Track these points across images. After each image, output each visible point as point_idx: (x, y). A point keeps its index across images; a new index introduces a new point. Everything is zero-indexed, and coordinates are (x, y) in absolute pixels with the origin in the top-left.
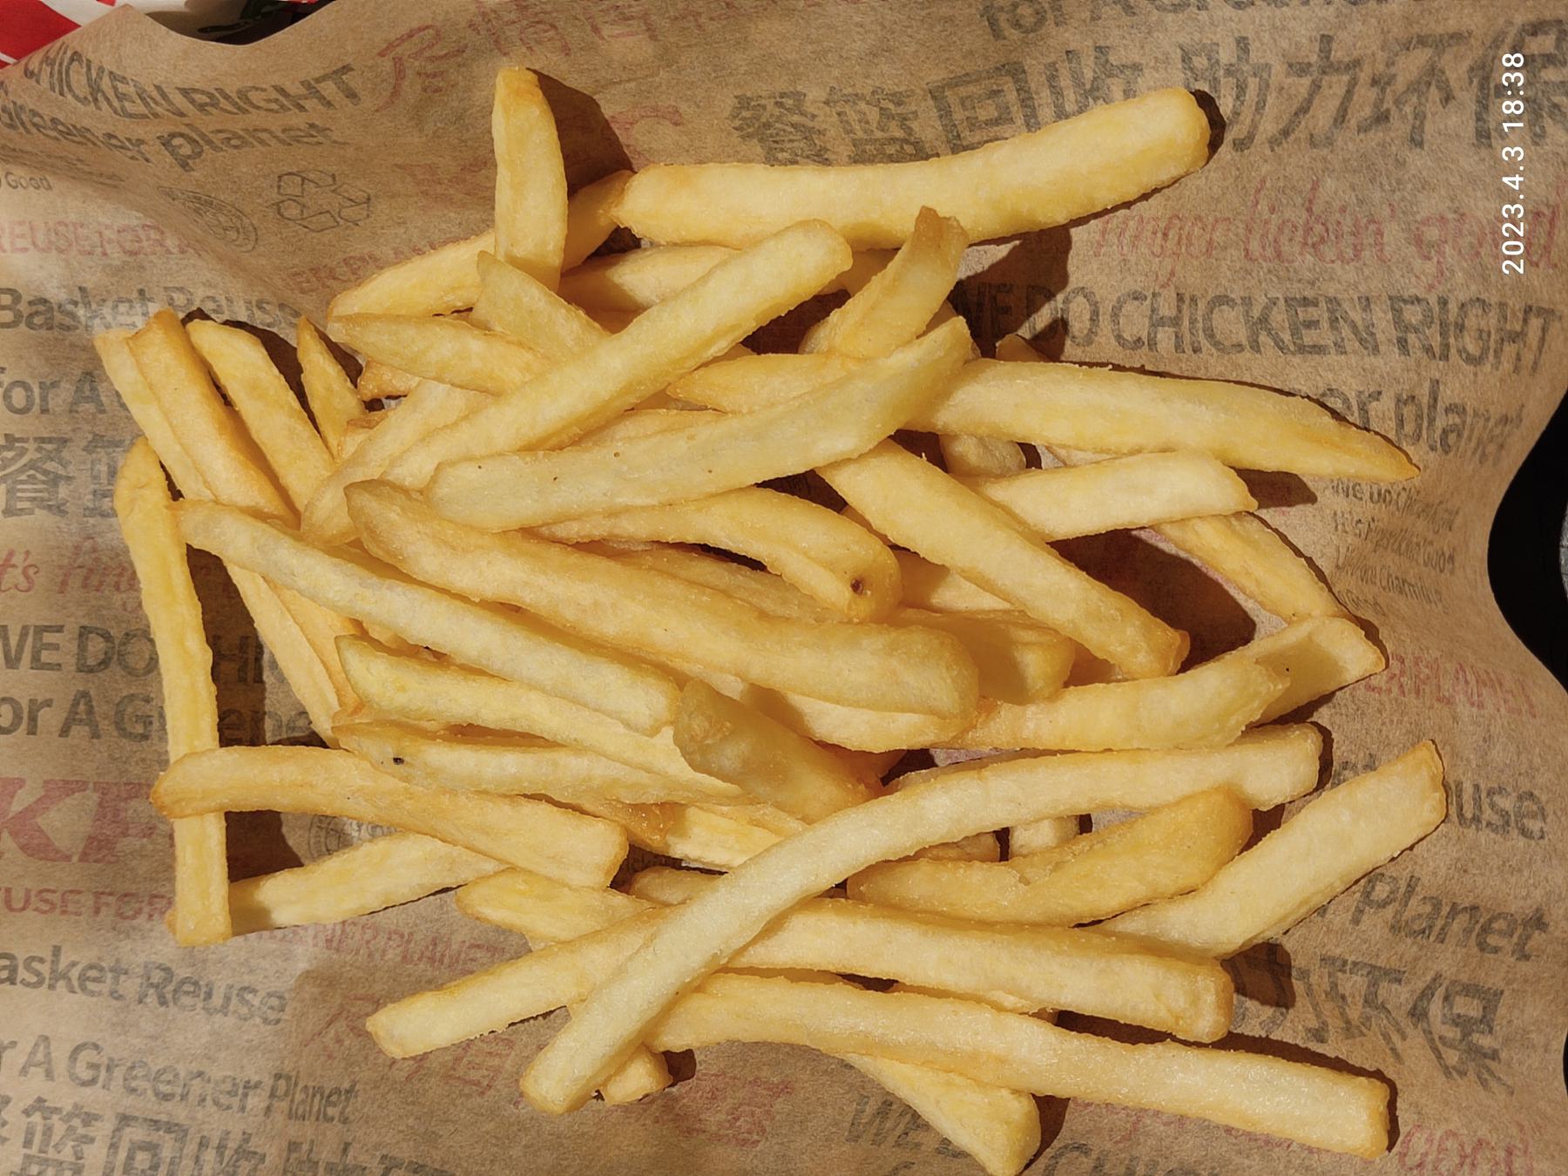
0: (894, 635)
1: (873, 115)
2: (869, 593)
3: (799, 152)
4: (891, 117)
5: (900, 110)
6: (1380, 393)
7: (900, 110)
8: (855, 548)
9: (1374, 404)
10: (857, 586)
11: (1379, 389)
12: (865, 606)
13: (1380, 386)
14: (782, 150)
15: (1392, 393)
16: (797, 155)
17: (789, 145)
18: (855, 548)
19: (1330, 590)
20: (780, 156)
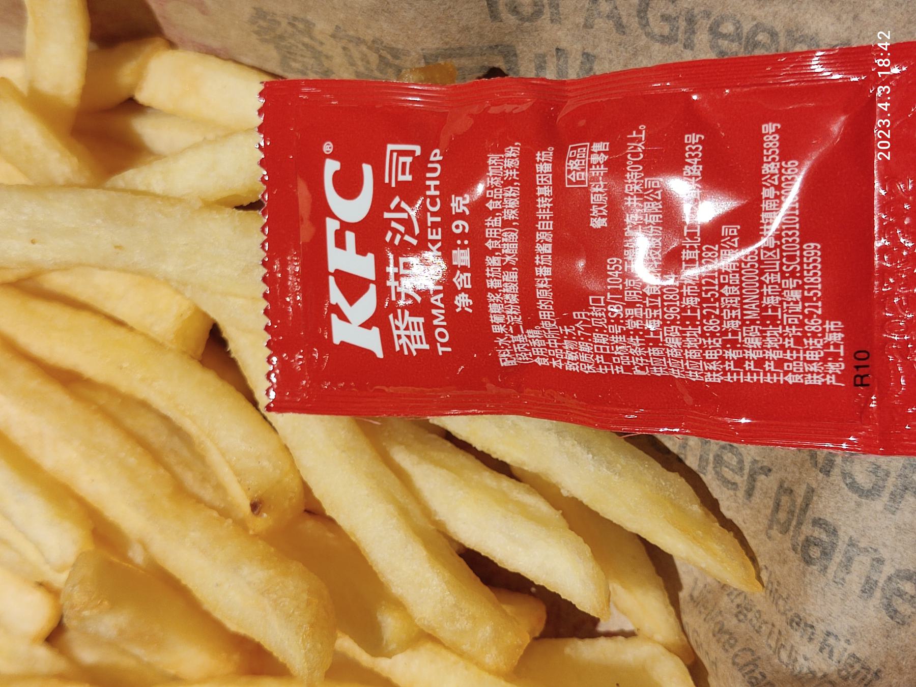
0: (272, 572)
1: (373, 58)
2: (265, 515)
3: (310, 67)
4: (388, 64)
5: (397, 62)
6: (770, 470)
7: (397, 62)
8: (265, 463)
9: (763, 477)
10: (255, 507)
11: (770, 466)
12: (262, 522)
13: (772, 464)
14: (295, 60)
15: (778, 476)
16: (307, 68)
17: (300, 59)
18: (265, 463)
19: (679, 616)
20: (293, 64)
